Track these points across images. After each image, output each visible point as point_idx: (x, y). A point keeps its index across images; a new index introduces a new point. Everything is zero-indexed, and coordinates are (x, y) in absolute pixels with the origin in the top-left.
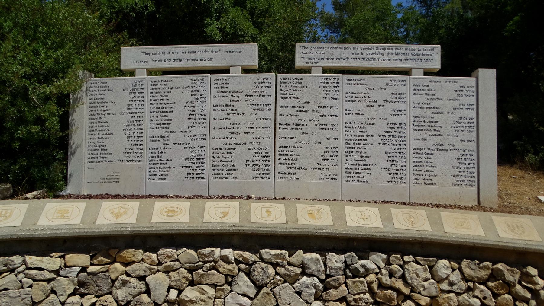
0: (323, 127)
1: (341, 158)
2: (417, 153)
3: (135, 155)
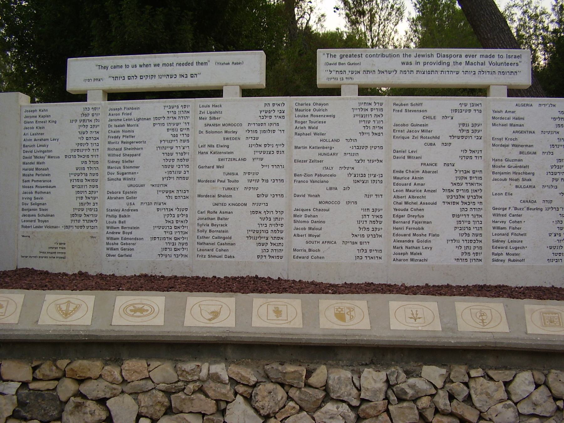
0: (360, 179)
1: (387, 225)
2: (498, 215)
3: (87, 218)
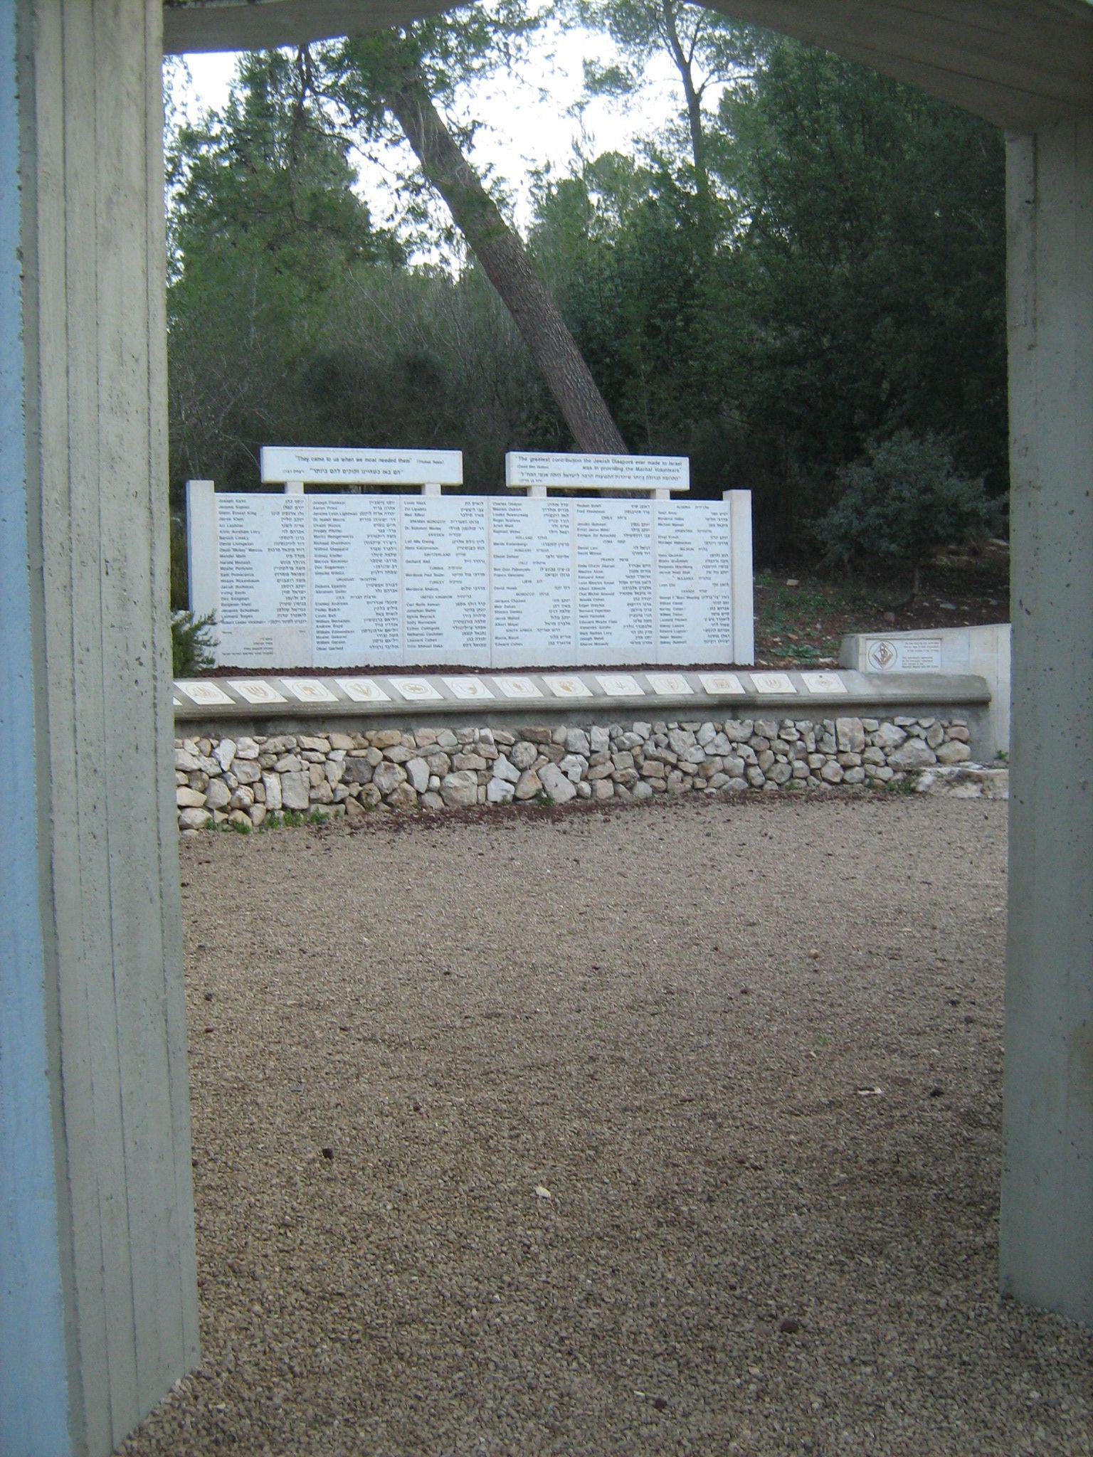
0: (551, 572)
